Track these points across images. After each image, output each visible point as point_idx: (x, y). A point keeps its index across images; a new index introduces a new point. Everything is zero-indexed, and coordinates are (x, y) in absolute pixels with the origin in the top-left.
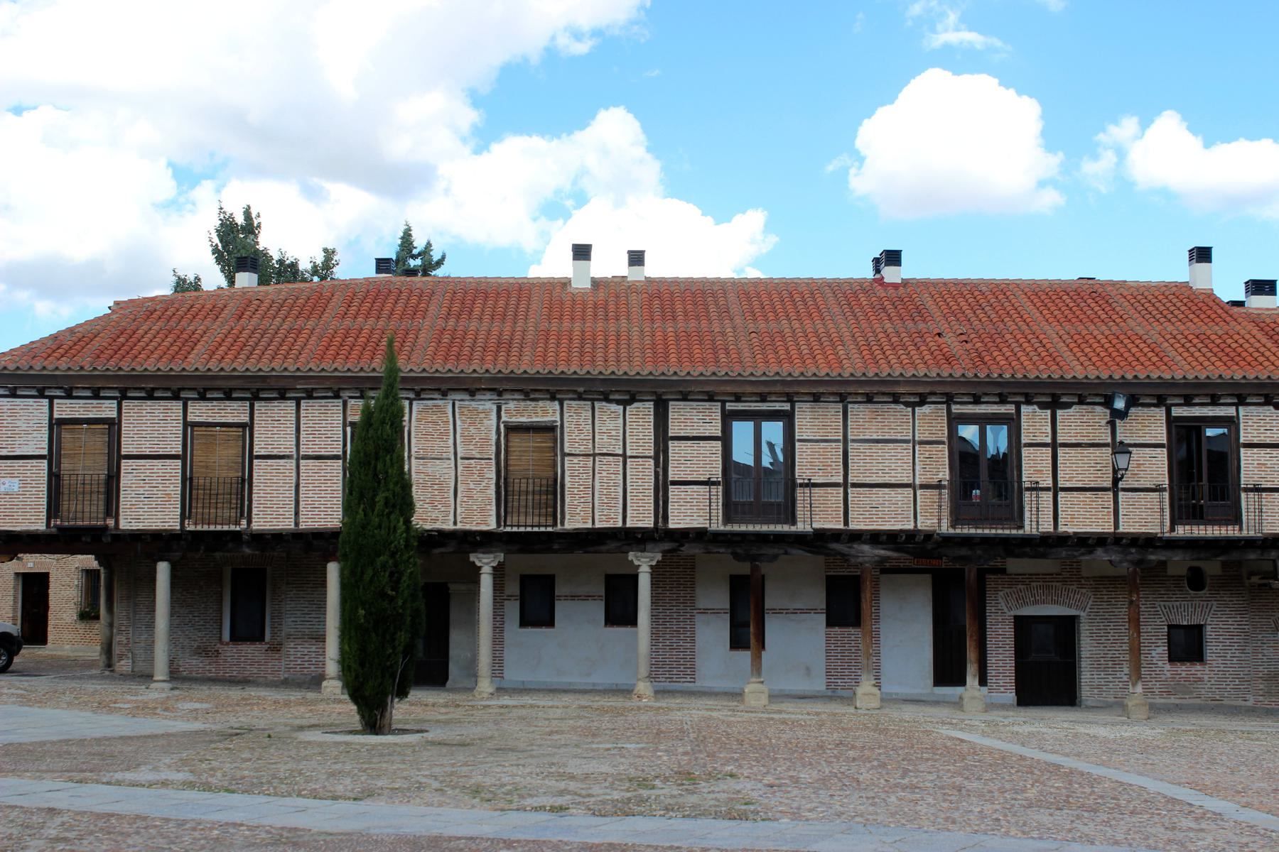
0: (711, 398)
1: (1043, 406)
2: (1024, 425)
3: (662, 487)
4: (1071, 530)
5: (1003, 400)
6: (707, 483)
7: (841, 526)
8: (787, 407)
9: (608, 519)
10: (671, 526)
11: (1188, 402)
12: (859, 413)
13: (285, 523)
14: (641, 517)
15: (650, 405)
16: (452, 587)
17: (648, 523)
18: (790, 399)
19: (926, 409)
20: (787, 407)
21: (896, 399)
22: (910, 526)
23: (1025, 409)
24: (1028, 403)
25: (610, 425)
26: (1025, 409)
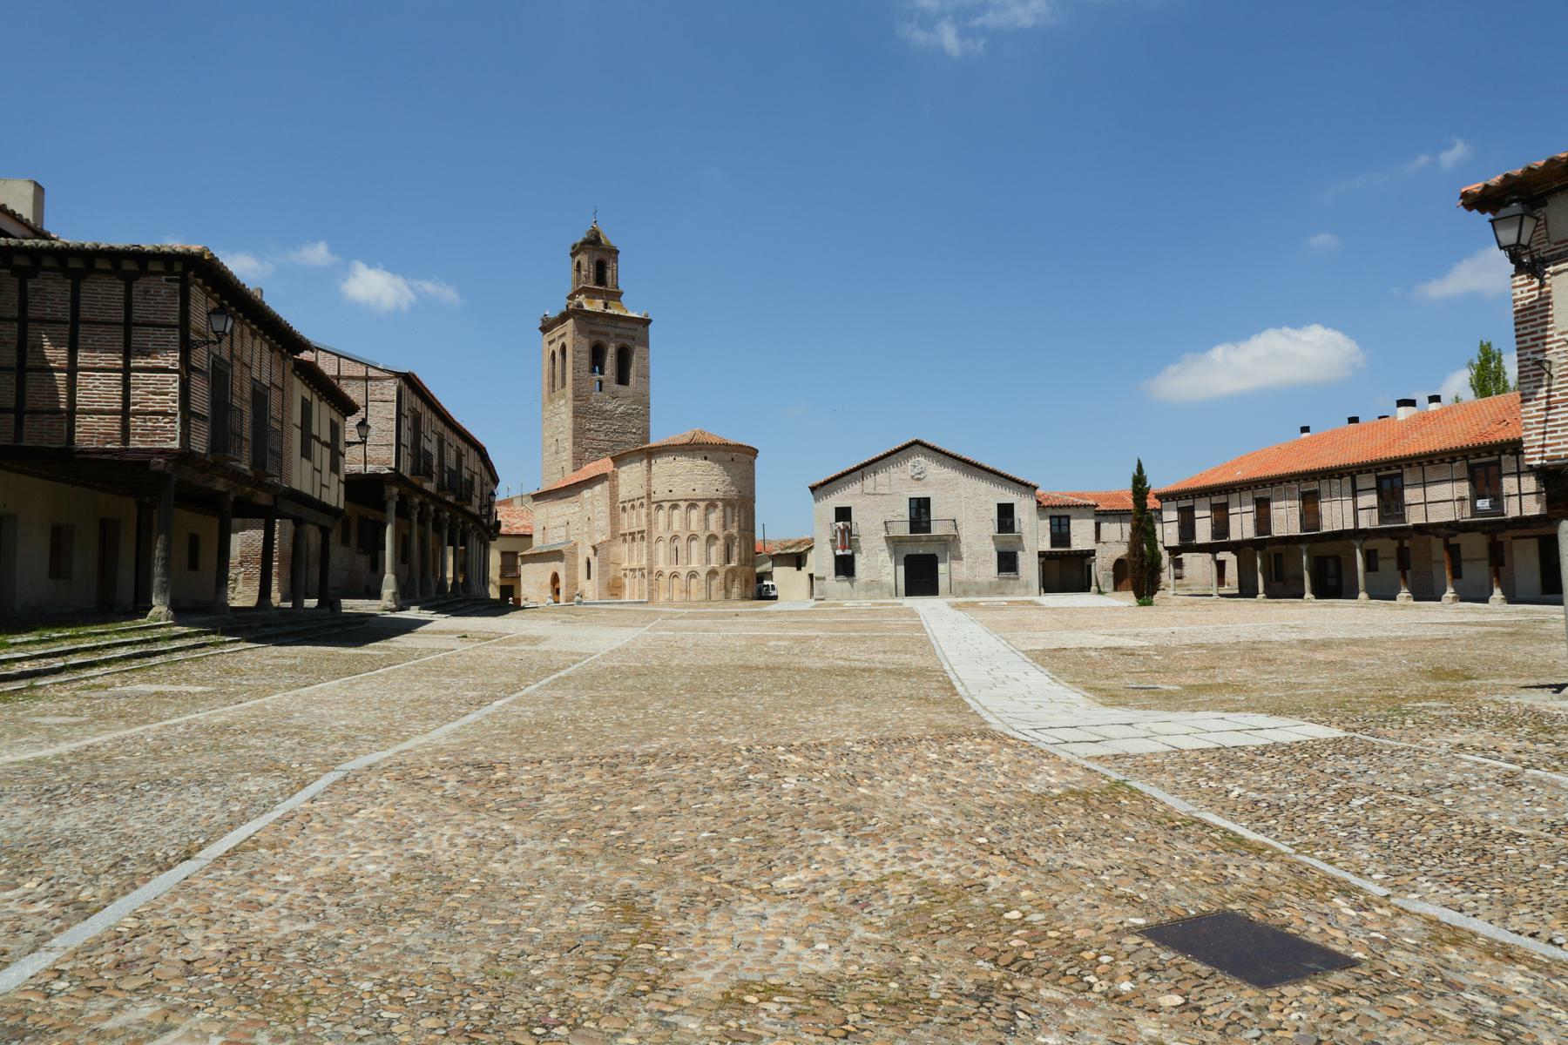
0: (1369, 471)
1: (1511, 454)
2: (1503, 465)
3: (1356, 510)
4: (1528, 514)
5: (1490, 454)
6: (1410, 505)
7: (1424, 522)
8: (1400, 471)
9: (1338, 527)
10: (1360, 527)
11: (1478, 456)
12: (1429, 469)
13: (1239, 538)
14: (1350, 526)
15: (1349, 478)
16: (1342, 557)
17: (1352, 527)
18: (1399, 467)
19: (1457, 464)
20: (1400, 471)
21: (1442, 461)
22: (1453, 519)
23: (1503, 457)
24: (1505, 454)
25: (1336, 488)
26: (1503, 457)
